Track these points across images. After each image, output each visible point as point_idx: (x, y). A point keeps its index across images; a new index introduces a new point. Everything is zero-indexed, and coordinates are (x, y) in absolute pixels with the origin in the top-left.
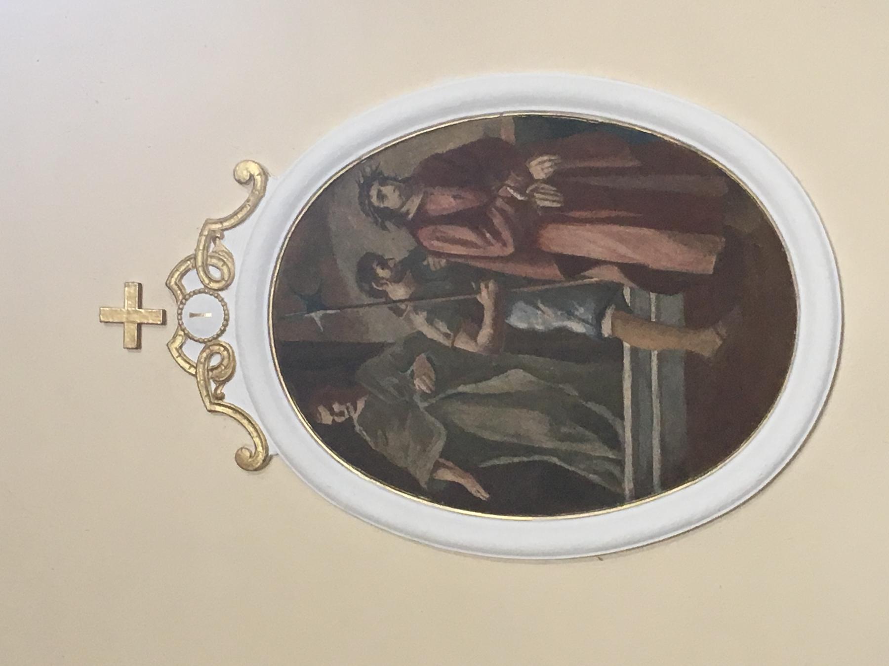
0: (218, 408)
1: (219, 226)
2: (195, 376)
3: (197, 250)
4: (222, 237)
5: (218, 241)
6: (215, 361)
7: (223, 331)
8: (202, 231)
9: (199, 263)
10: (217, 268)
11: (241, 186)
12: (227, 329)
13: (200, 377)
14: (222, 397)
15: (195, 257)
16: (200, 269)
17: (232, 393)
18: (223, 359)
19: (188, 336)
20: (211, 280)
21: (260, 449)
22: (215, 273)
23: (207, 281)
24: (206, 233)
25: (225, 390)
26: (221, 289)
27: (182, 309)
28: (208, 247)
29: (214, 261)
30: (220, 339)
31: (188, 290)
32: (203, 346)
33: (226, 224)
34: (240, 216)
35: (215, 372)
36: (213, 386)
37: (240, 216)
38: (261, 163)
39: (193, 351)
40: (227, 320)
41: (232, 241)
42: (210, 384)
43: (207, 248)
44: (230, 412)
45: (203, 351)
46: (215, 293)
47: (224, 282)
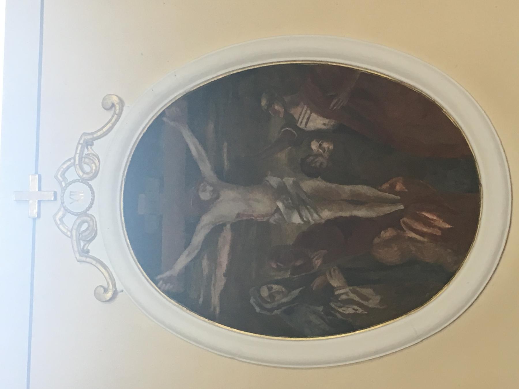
0: (84, 259)
1: (90, 137)
2: (71, 237)
3: (76, 153)
4: (92, 145)
5: (89, 147)
6: (85, 226)
7: (90, 207)
8: (79, 141)
9: (77, 162)
10: (88, 164)
11: (105, 111)
12: (93, 206)
13: (74, 238)
14: (88, 252)
15: (74, 158)
16: (78, 167)
17: (95, 248)
18: (89, 226)
19: (67, 210)
20: (84, 173)
21: (111, 287)
22: (87, 168)
23: (81, 174)
24: (82, 142)
25: (90, 247)
26: (92, 179)
27: (64, 193)
28: (84, 150)
29: (87, 160)
30: (88, 212)
31: (70, 180)
32: (76, 217)
33: (95, 135)
34: (105, 130)
35: (83, 235)
36: (82, 244)
37: (105, 130)
38: (120, 96)
39: (70, 220)
40: (93, 200)
41: (98, 147)
42: (80, 244)
43: (82, 151)
44: (94, 262)
45: (77, 219)
46: (85, 181)
47: (91, 175)
